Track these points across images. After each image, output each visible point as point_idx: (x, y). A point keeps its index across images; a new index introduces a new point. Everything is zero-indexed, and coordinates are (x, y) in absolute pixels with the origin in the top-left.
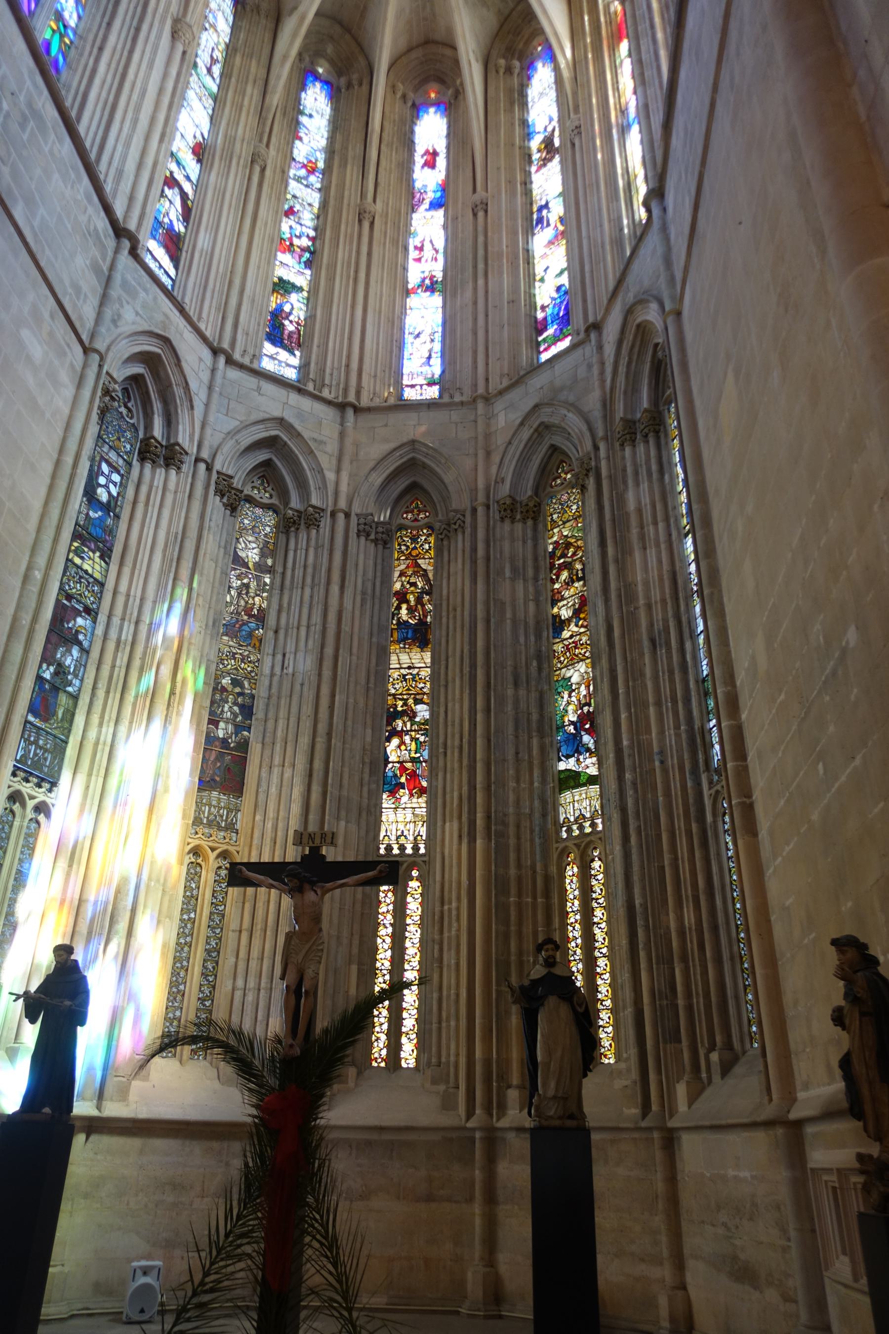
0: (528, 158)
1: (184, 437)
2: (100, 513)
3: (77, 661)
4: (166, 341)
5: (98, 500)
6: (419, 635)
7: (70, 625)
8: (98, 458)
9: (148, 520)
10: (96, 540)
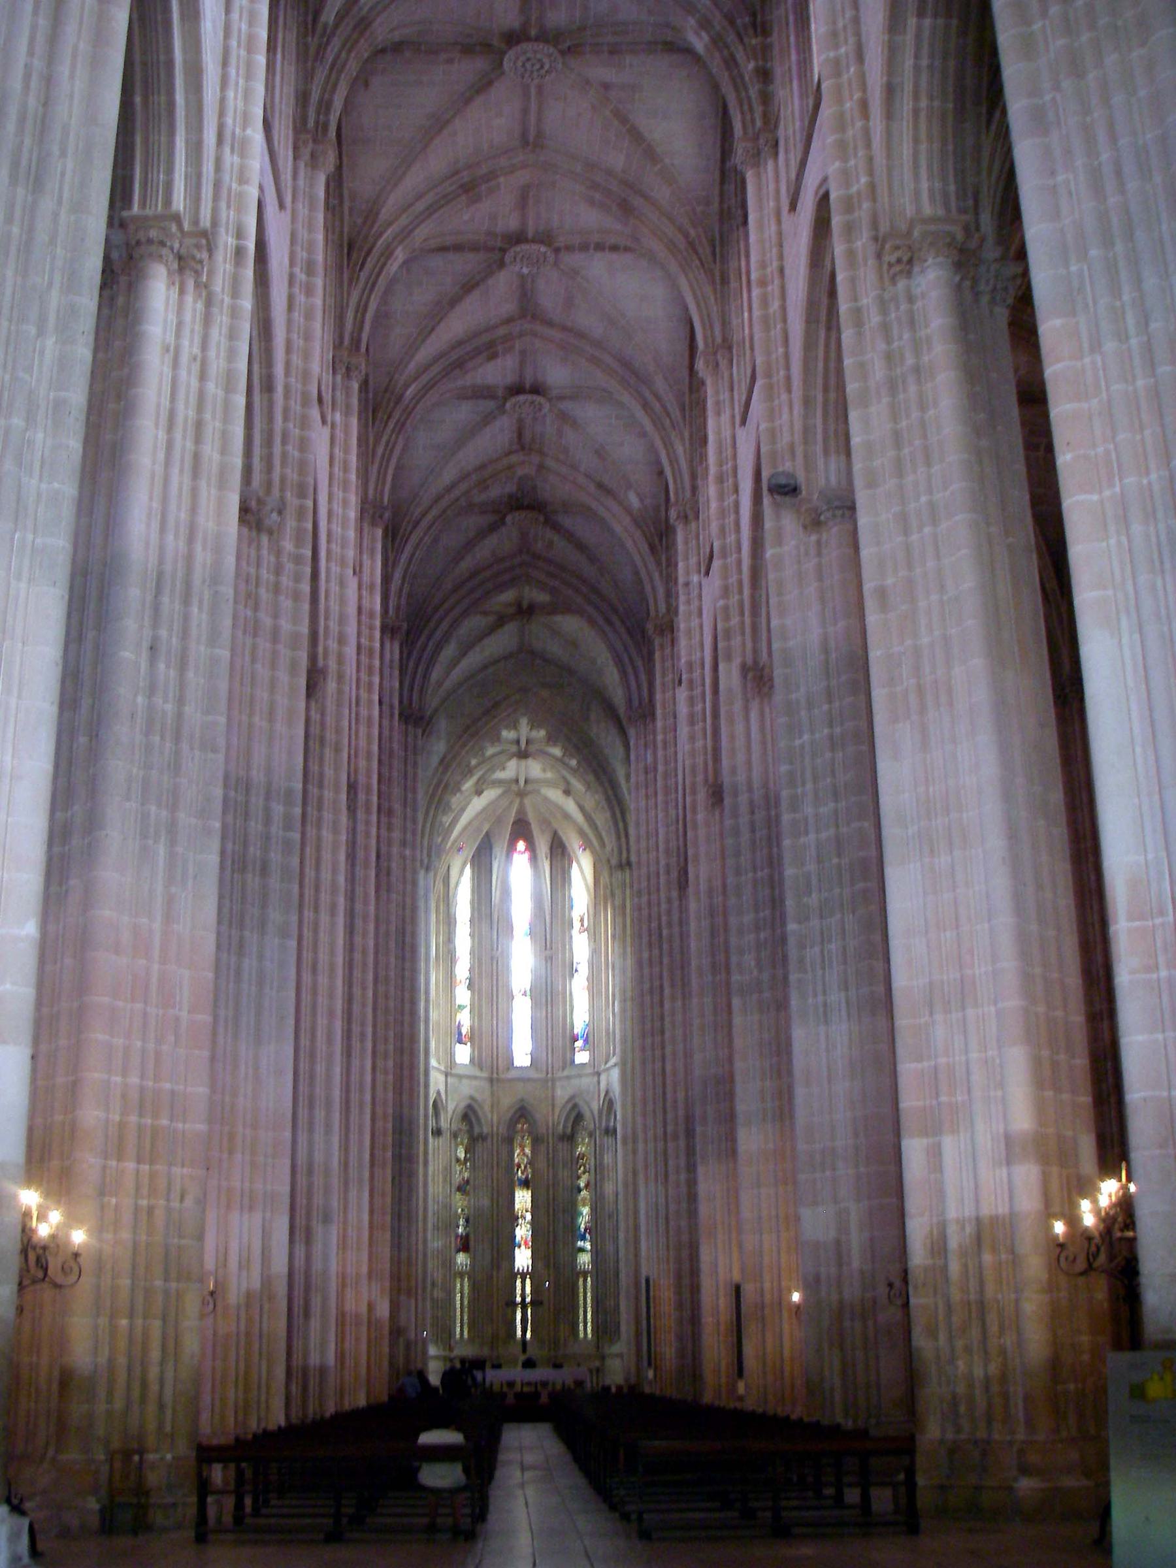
0: (571, 926)
4: (438, 1093)
6: (526, 1184)
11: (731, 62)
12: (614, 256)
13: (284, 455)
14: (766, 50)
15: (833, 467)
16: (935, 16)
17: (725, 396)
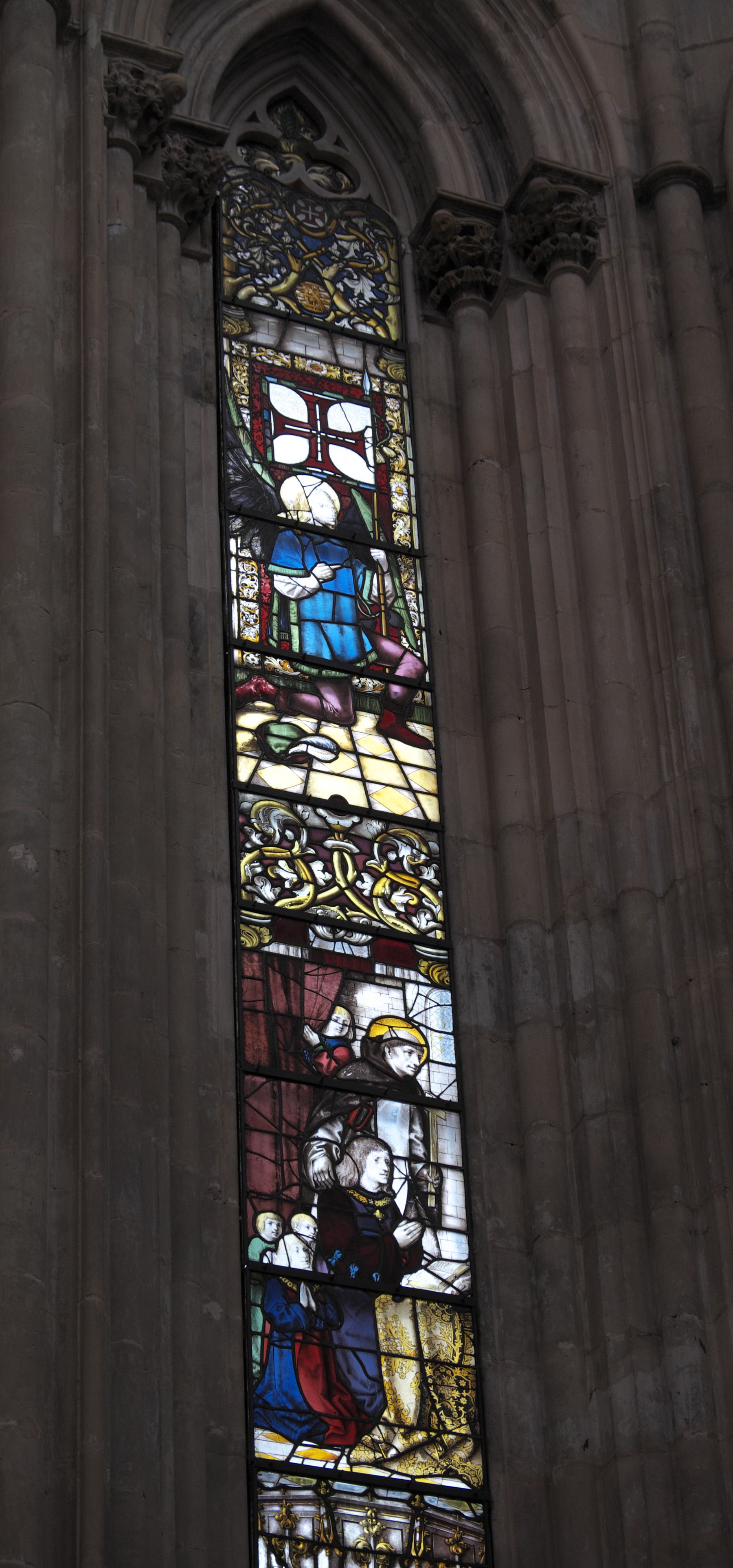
1: (555, 135)
2: (322, 570)
3: (411, 1159)
5: (295, 525)
7: (333, 1030)
8: (241, 380)
9: (531, 509)
10: (340, 671)
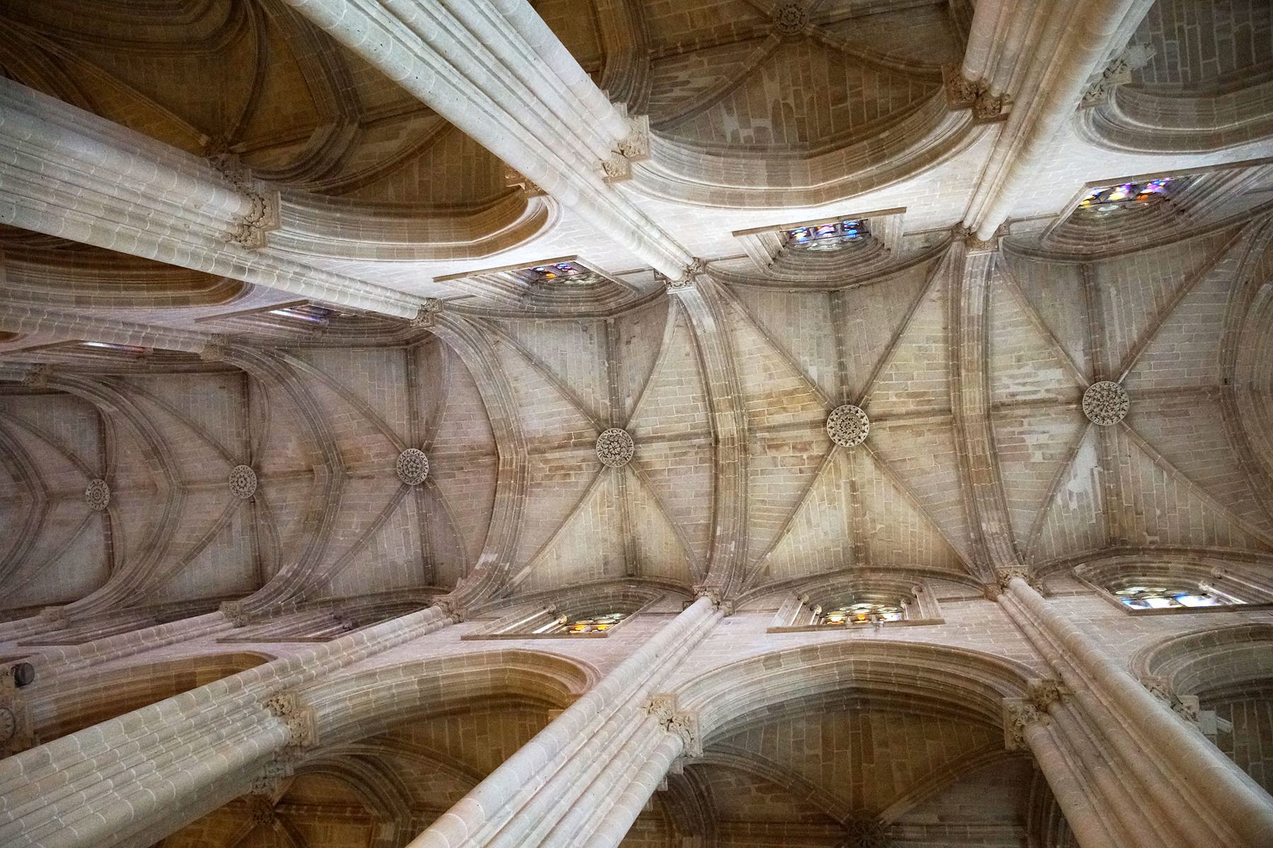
11: (278, 592)
12: (101, 547)
13: (24, 310)
14: (289, 611)
15: (46, 708)
16: (421, 691)
17: (31, 630)
